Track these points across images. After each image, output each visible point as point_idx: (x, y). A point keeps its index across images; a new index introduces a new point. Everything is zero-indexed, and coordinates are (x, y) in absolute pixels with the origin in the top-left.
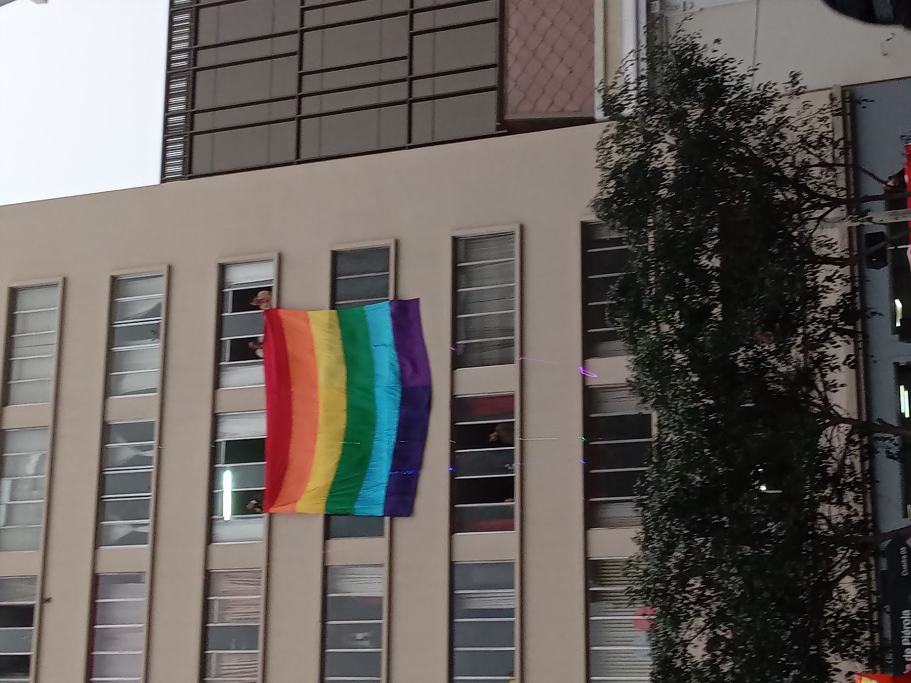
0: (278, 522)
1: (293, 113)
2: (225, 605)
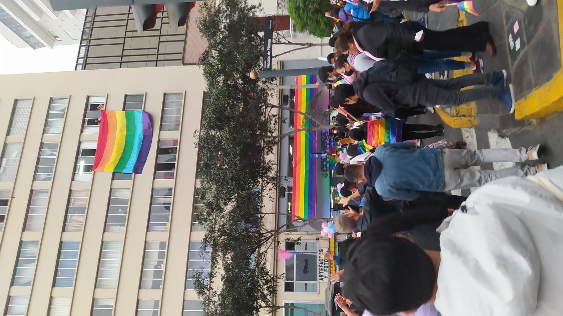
0: (97, 174)
1: (120, 61)
2: (75, 200)
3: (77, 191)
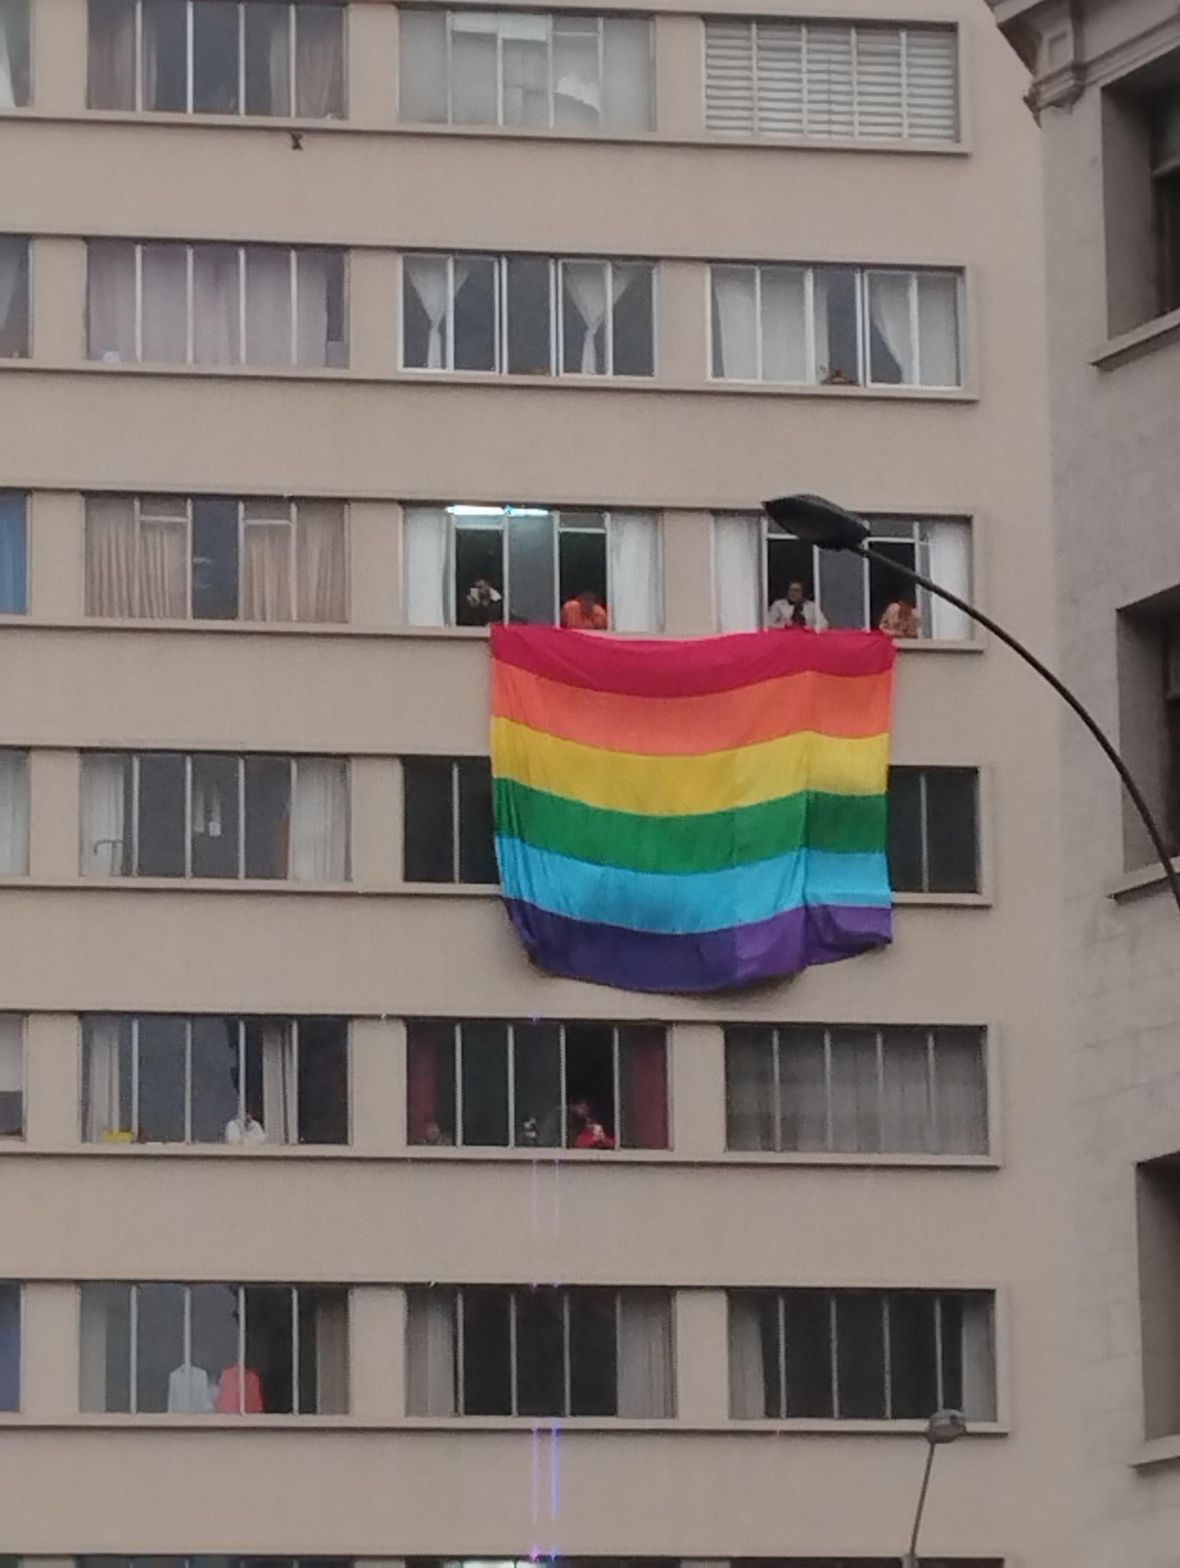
3: (337, 549)
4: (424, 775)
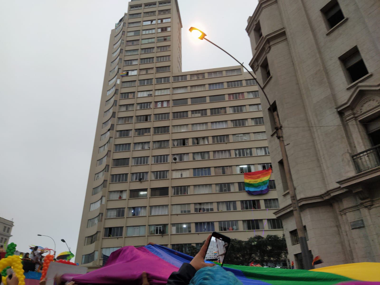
2: (228, 168)
3: (232, 169)
4: (239, 183)
